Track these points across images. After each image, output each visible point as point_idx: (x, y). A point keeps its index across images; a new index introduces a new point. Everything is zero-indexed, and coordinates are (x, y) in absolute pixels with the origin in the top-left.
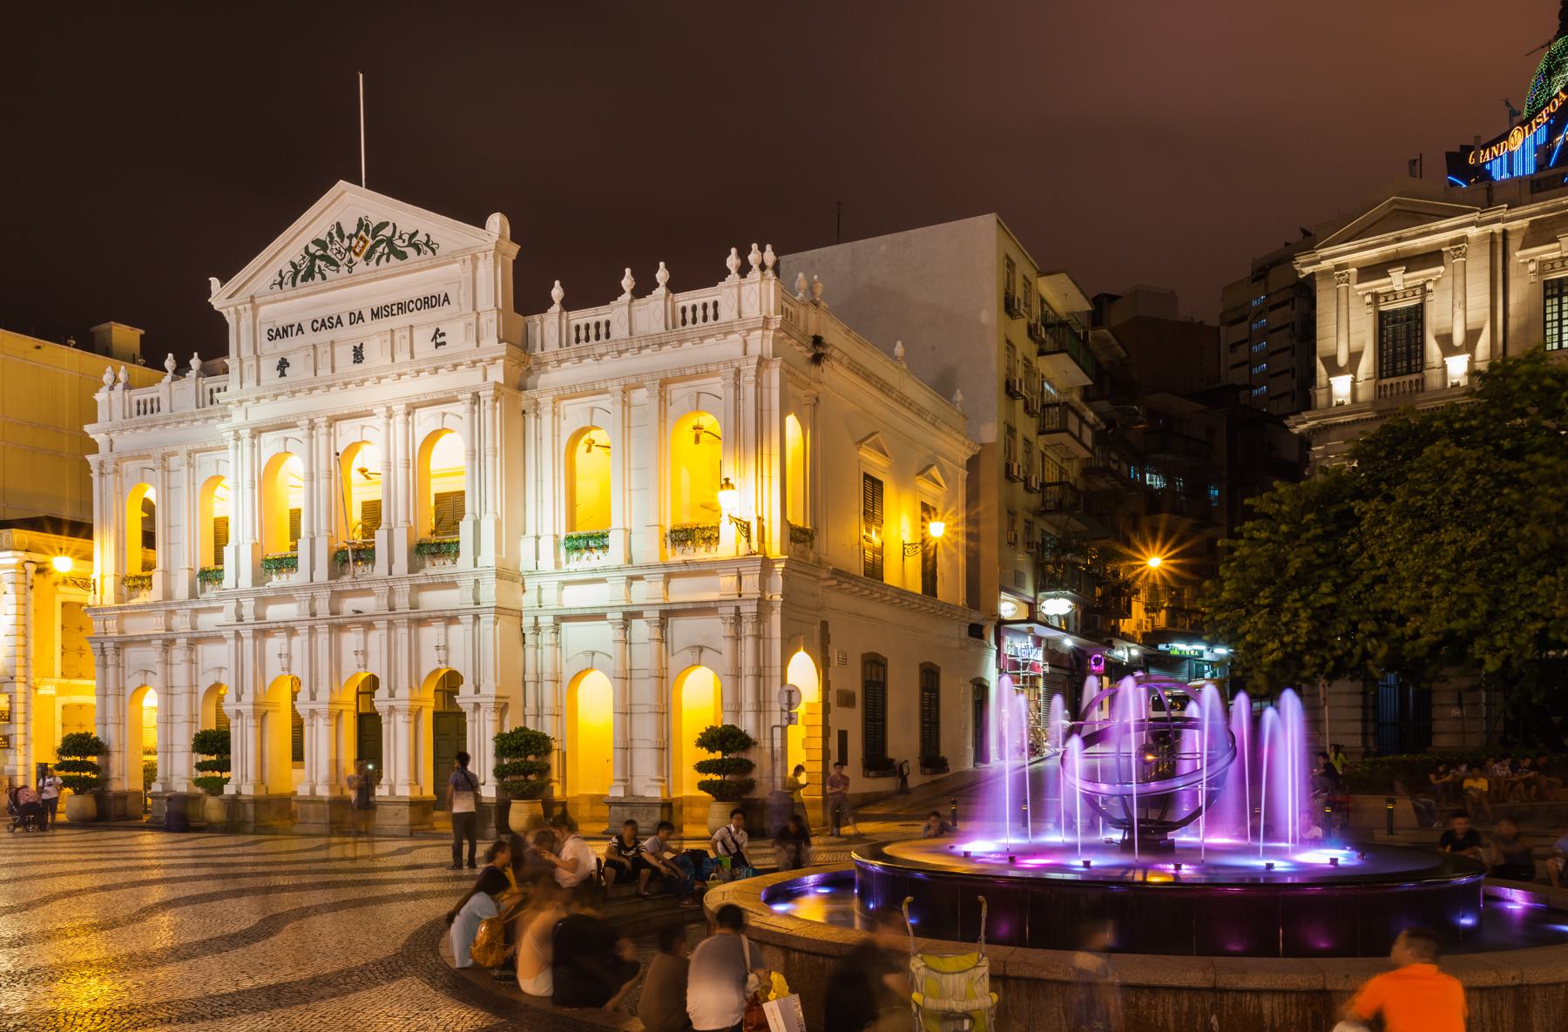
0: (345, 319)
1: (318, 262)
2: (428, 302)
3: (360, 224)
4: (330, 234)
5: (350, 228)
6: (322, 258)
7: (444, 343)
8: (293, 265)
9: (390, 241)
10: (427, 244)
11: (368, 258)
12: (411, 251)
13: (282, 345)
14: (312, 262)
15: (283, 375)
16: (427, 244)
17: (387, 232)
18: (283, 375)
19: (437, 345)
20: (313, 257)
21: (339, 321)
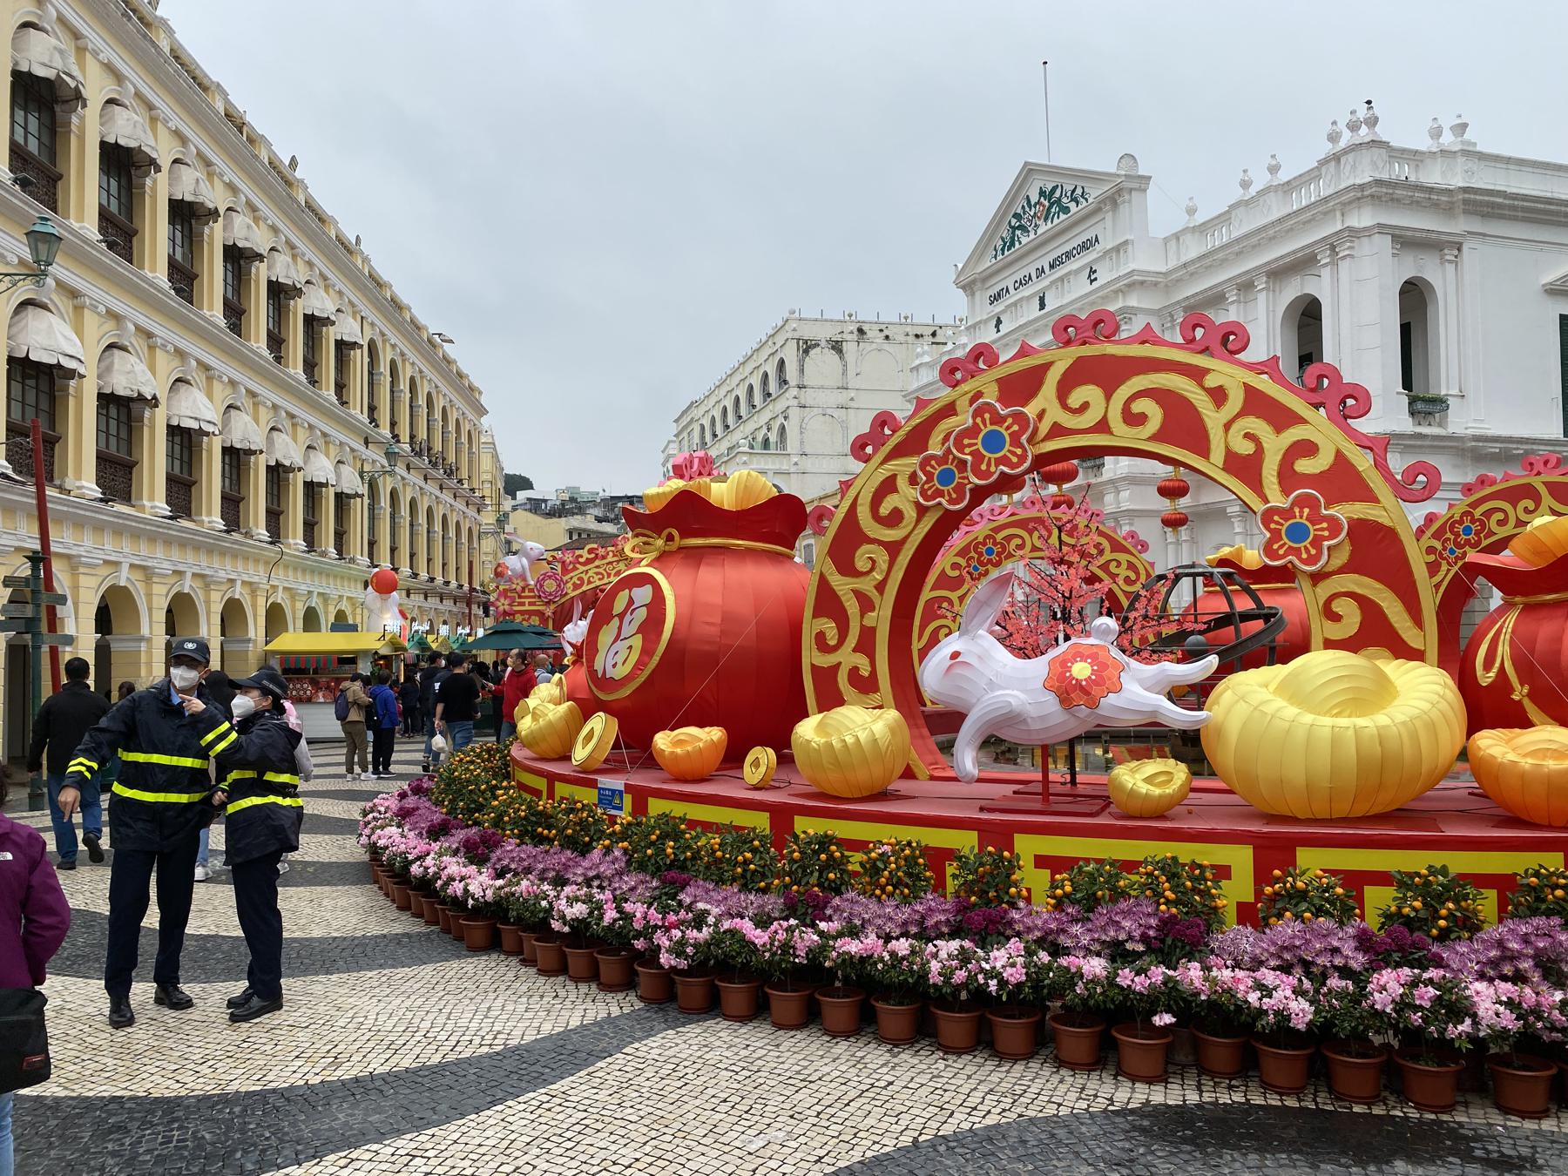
0: (1034, 277)
1: (1018, 232)
2: (1085, 247)
3: (1042, 193)
4: (1023, 207)
5: (1034, 199)
6: (1019, 227)
7: (1096, 279)
8: (1003, 239)
9: (1059, 199)
10: (1082, 196)
11: (1046, 220)
12: (1072, 205)
13: (999, 307)
14: (1013, 233)
15: (998, 331)
16: (1082, 196)
17: (1057, 194)
18: (998, 331)
19: (1092, 281)
20: (1014, 228)
21: (1030, 278)
